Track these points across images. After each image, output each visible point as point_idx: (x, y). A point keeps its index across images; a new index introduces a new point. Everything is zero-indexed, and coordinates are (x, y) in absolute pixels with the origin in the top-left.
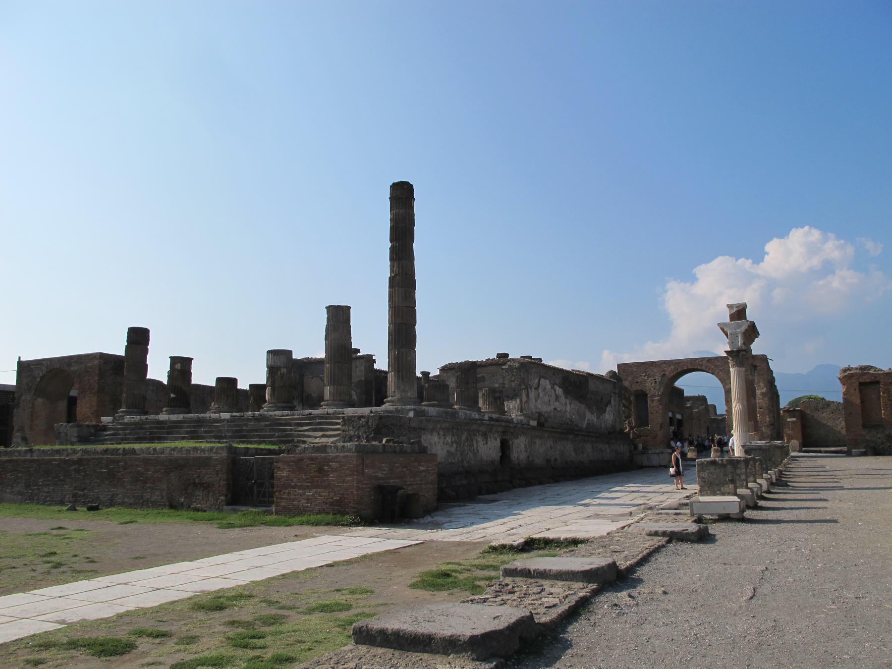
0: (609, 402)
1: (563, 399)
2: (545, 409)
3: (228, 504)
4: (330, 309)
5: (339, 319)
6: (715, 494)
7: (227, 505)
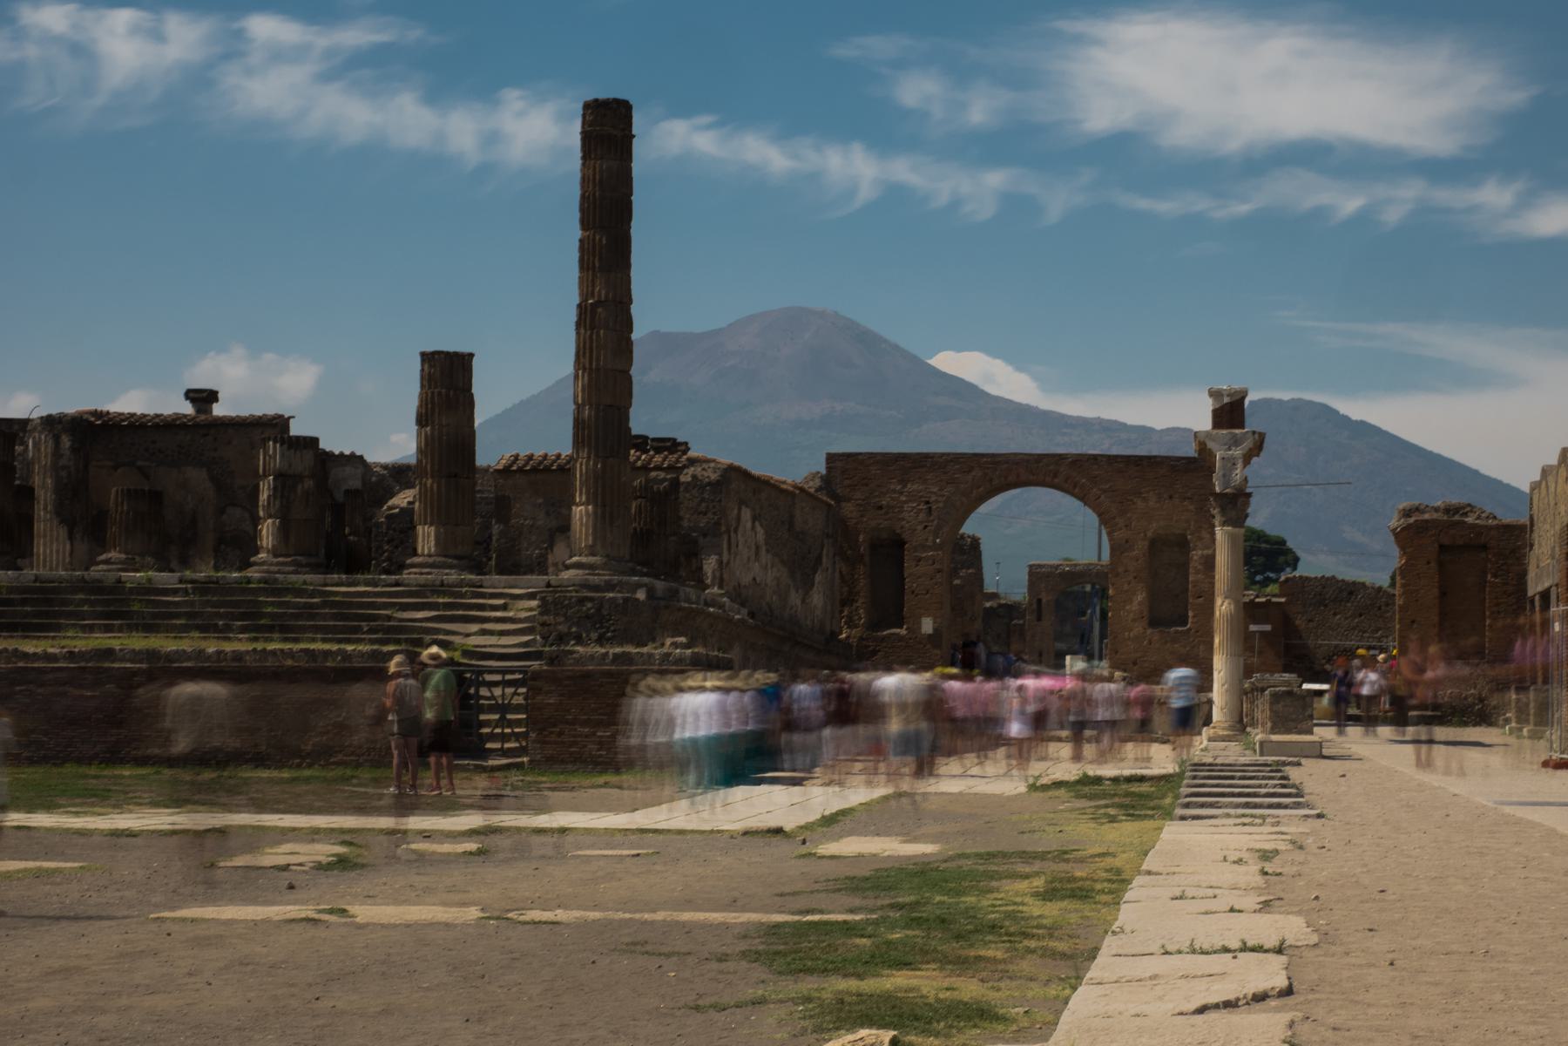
0: (819, 559)
1: (765, 557)
2: (746, 579)
4: (428, 358)
5: (447, 381)
6: (1288, 732)
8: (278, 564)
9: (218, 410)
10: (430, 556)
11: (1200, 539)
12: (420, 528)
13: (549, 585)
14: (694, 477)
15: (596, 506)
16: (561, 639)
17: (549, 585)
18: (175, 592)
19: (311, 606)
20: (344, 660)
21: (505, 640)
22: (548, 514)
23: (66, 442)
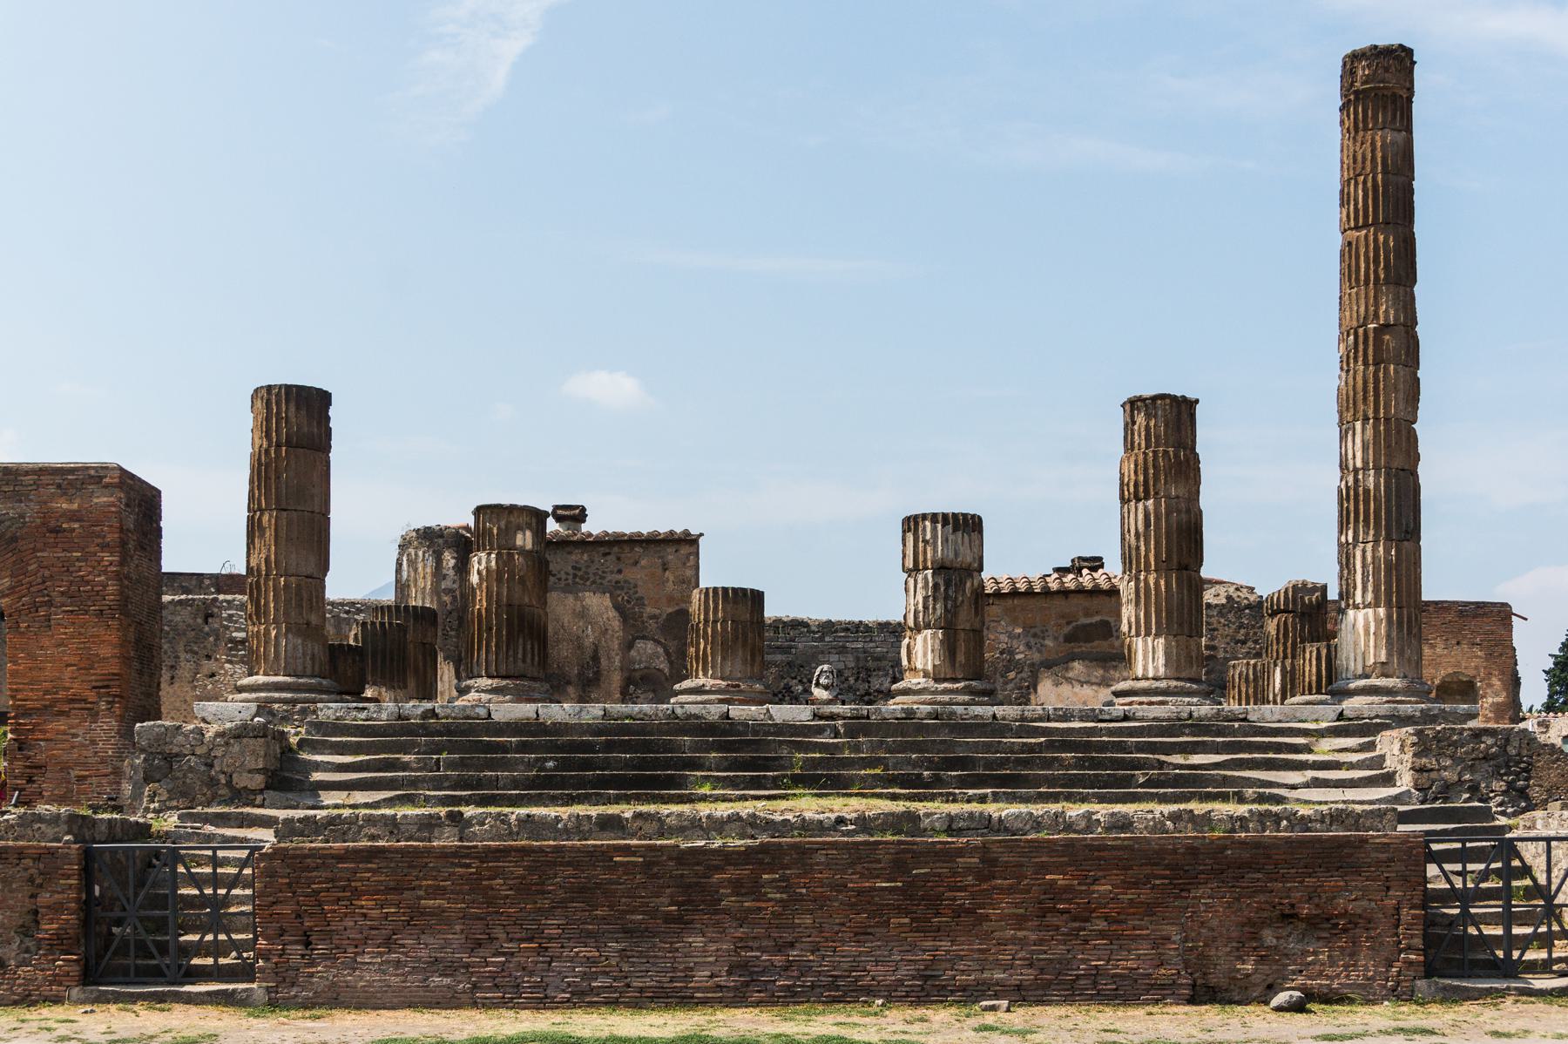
3: (1429, 972)
7: (1428, 975)
8: (945, 692)
9: (585, 528)
10: (1155, 679)
11: (1490, 685)
12: (1139, 644)
13: (1341, 716)
14: (1229, 598)
15: (1389, 605)
16: (1447, 791)
17: (1341, 716)
18: (819, 731)
19: (1031, 748)
20: (1291, 828)
21: (1351, 794)
22: (1029, 646)
23: (449, 560)
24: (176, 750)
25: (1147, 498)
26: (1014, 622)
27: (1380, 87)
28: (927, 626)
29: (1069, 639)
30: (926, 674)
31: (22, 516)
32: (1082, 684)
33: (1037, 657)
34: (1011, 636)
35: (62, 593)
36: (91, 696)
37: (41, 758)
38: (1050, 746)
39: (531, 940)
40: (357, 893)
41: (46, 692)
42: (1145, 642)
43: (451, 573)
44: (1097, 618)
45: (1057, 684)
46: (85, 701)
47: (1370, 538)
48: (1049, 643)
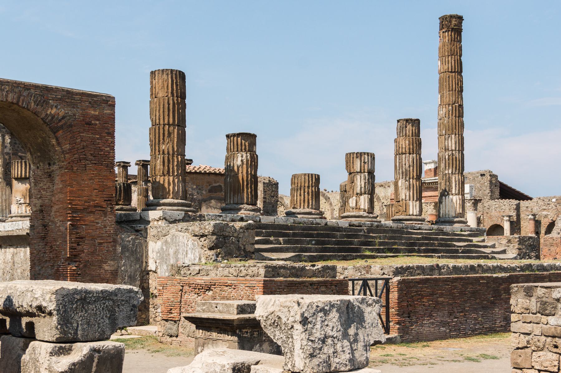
10: (413, 215)
22: (198, 193)
24: (227, 234)
25: (413, 154)
26: (193, 183)
27: (453, 26)
28: (365, 193)
29: (210, 191)
30: (365, 211)
31: (74, 115)
32: (215, 208)
33: (200, 197)
34: (193, 189)
35: (91, 154)
36: (104, 204)
37: (83, 233)
38: (423, 238)
39: (462, 312)
40: (423, 297)
41: (86, 202)
42: (413, 203)
43: (9, 145)
44: (218, 184)
45: (207, 208)
46: (102, 207)
47: (457, 173)
48: (204, 192)
